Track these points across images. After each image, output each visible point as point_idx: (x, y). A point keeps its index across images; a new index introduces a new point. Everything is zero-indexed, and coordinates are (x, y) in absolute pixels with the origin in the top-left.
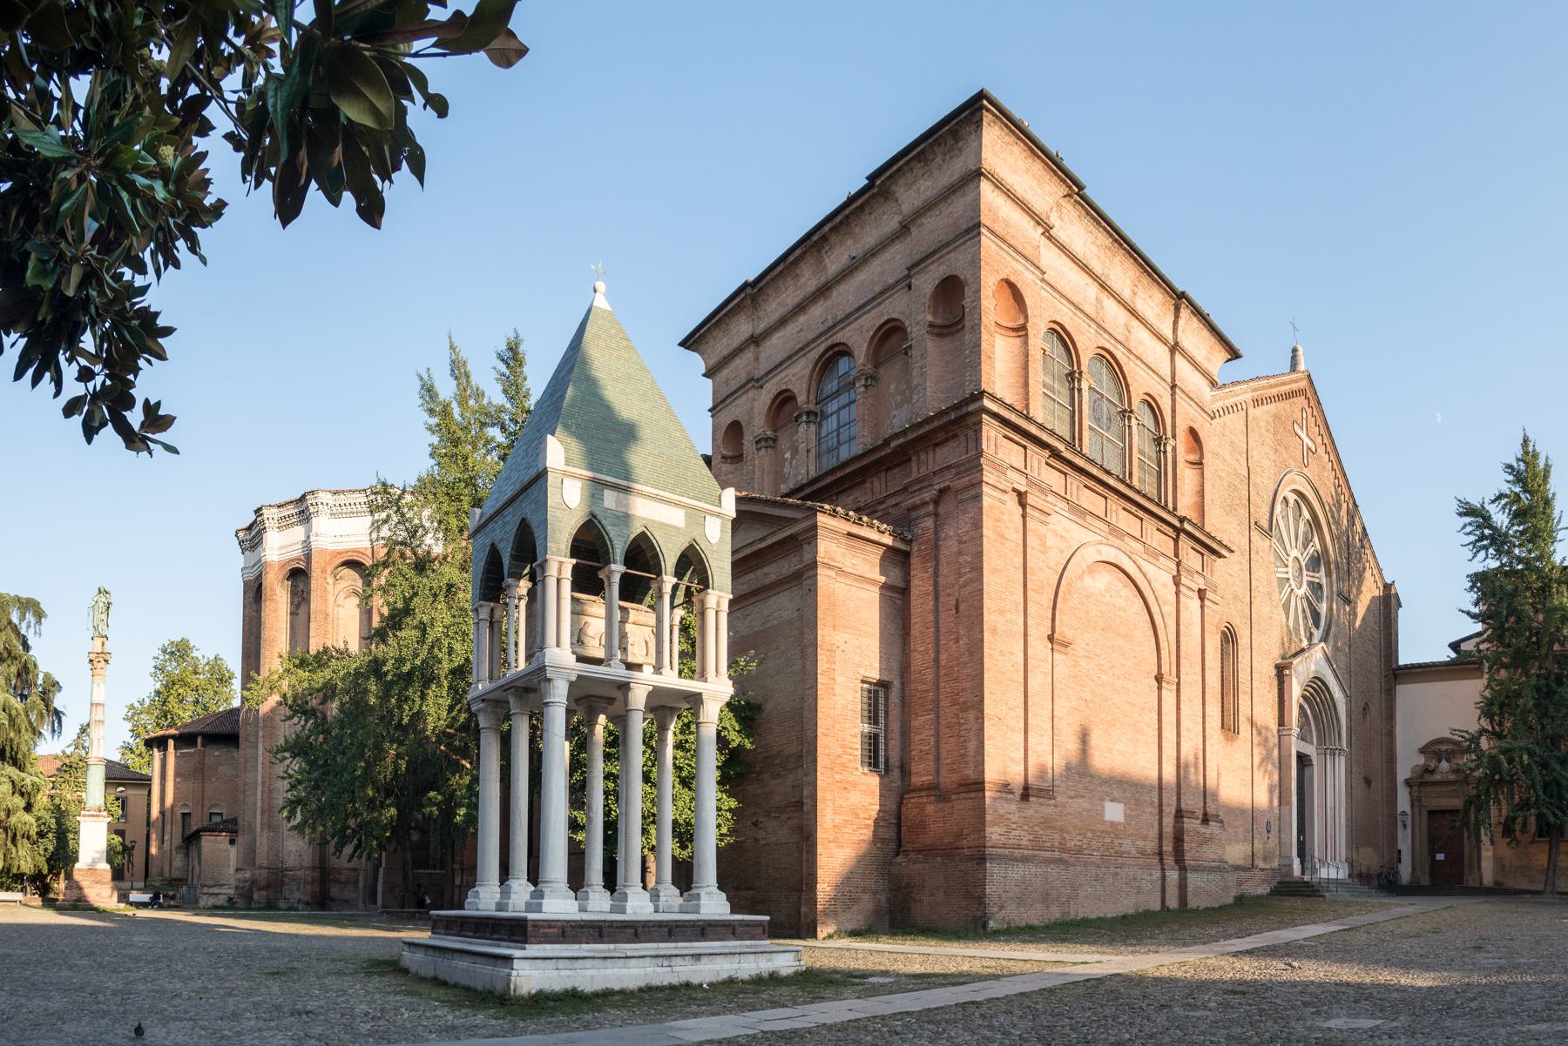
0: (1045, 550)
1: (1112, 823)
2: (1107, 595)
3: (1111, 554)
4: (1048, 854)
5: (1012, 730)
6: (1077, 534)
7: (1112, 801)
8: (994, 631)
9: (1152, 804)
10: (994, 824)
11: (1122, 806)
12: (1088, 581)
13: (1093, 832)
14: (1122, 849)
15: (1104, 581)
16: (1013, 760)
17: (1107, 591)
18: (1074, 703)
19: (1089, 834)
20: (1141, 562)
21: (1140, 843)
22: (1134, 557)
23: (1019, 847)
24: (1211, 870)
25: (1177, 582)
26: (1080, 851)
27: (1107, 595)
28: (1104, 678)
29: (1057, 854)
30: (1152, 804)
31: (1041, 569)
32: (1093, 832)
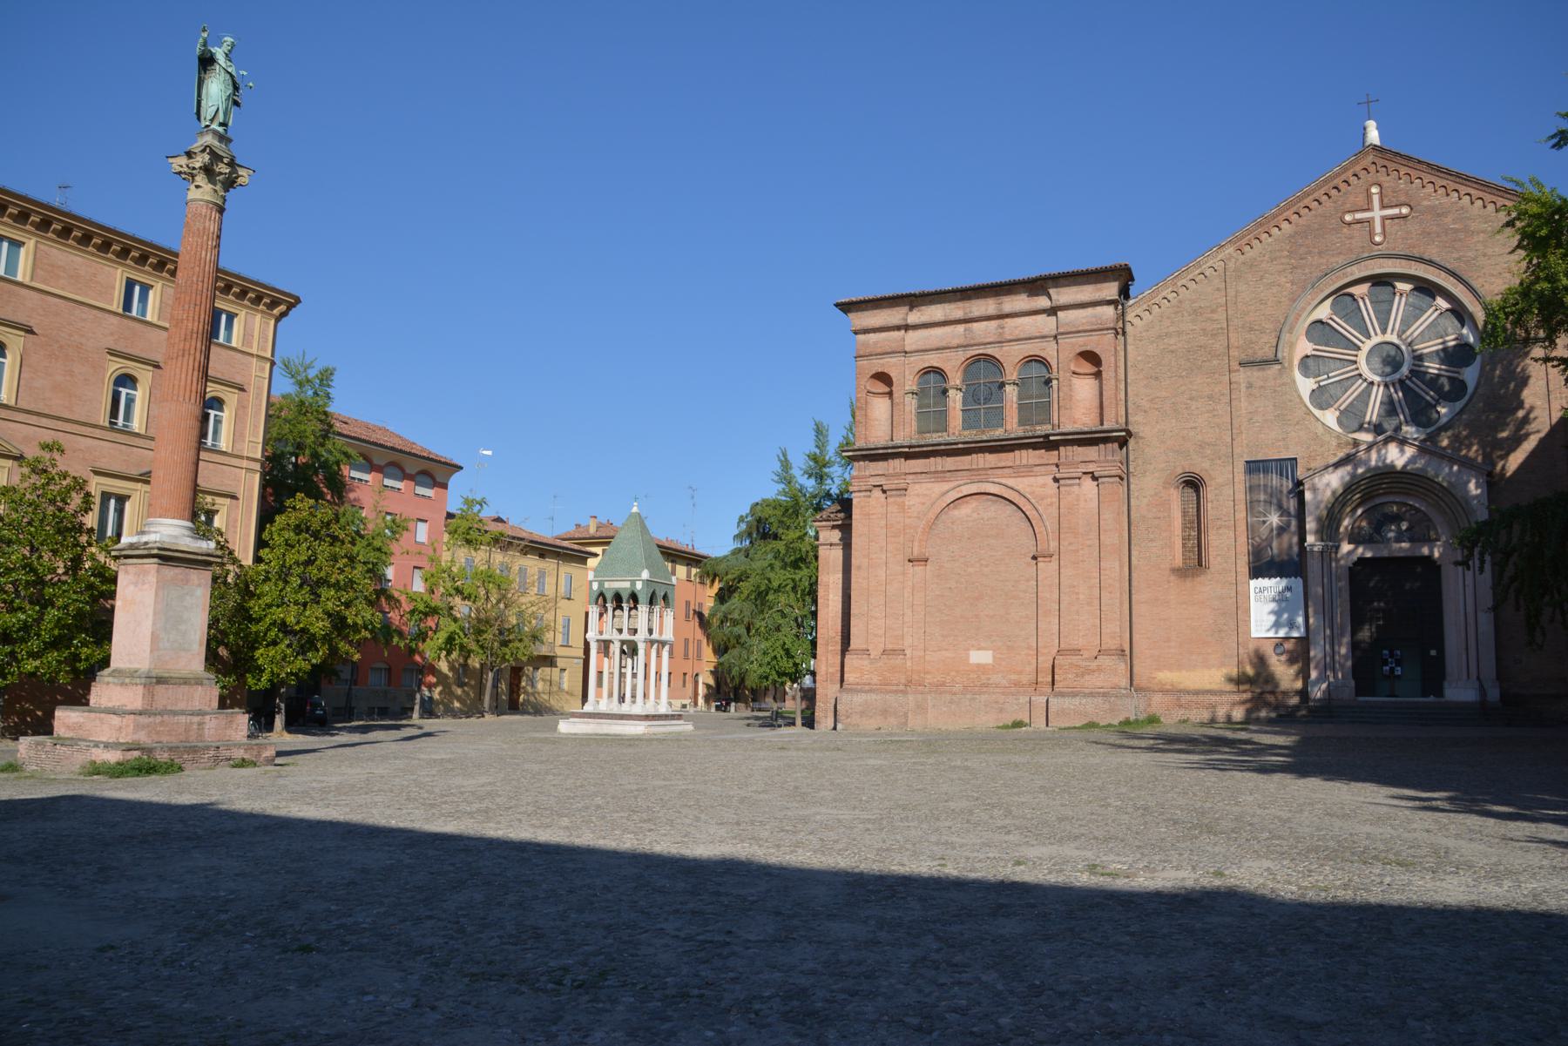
0: (902, 508)
1: (978, 666)
2: (975, 515)
3: (973, 488)
4: (895, 688)
5: (876, 618)
6: (939, 488)
7: (979, 649)
8: (859, 568)
9: (1029, 648)
10: (850, 672)
11: (991, 652)
12: (956, 513)
13: (957, 672)
14: (991, 682)
15: (965, 510)
16: (876, 635)
17: (973, 512)
18: (937, 593)
19: (953, 673)
20: (1003, 481)
21: (1014, 677)
22: (996, 480)
23: (869, 684)
24: (1091, 695)
25: (1056, 480)
26: (943, 684)
27: (975, 515)
28: (971, 570)
29: (902, 687)
30: (1029, 648)
31: (899, 522)
32: (957, 672)
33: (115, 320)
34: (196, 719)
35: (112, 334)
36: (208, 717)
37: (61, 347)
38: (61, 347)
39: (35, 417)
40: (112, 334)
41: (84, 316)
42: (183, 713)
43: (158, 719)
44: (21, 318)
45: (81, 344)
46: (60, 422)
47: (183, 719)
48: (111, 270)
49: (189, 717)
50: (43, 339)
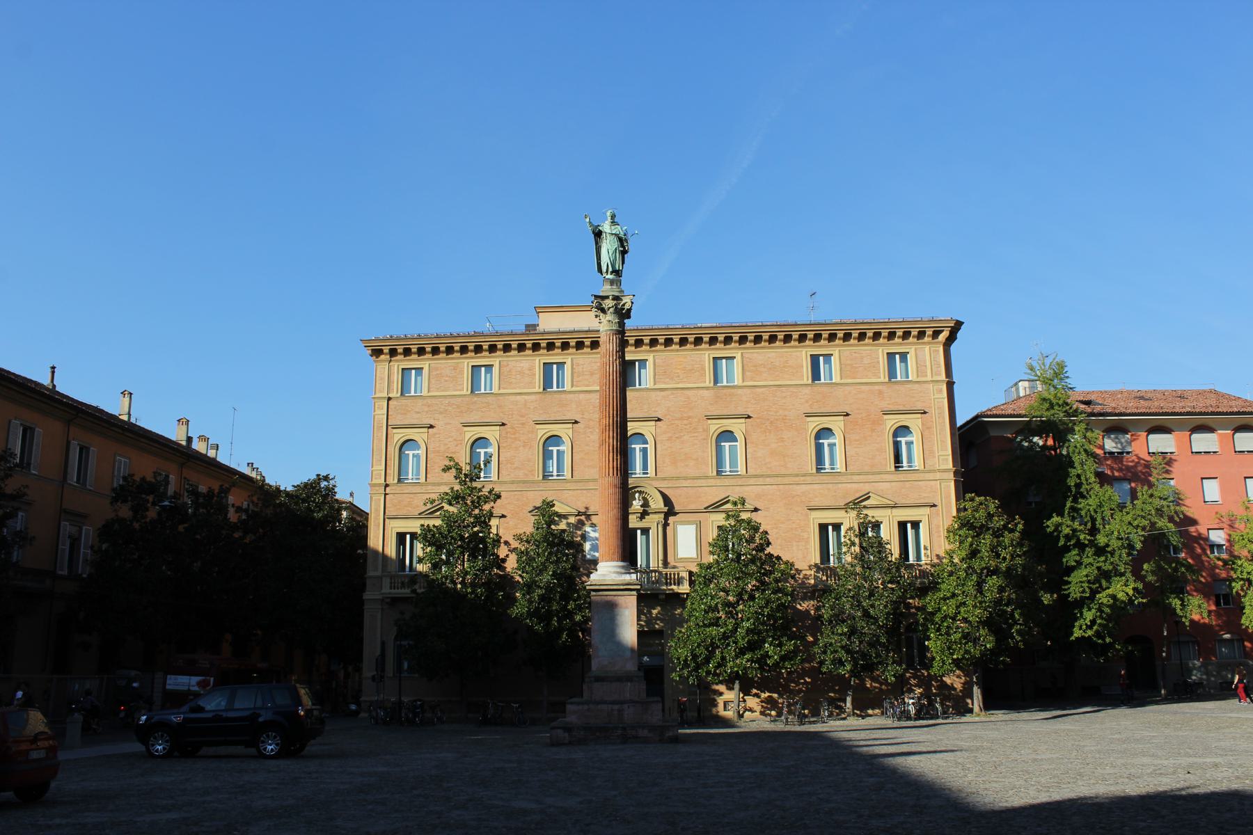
33: (807, 390)
34: (616, 707)
35: (807, 402)
36: (626, 706)
37: (771, 422)
38: (771, 422)
39: (761, 479)
40: (807, 402)
41: (784, 395)
42: (605, 702)
43: (586, 707)
44: (741, 411)
45: (785, 416)
46: (779, 478)
47: (604, 707)
48: (798, 354)
49: (610, 706)
50: (758, 420)
